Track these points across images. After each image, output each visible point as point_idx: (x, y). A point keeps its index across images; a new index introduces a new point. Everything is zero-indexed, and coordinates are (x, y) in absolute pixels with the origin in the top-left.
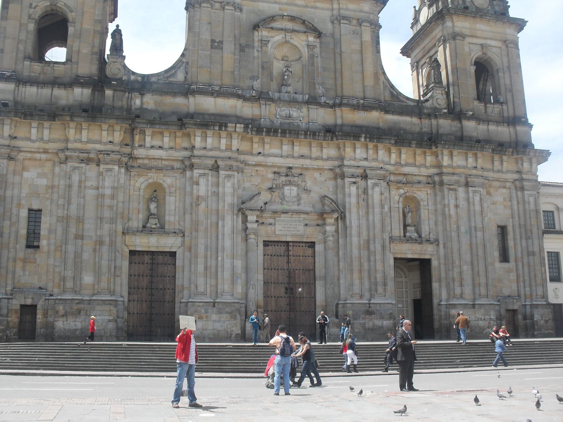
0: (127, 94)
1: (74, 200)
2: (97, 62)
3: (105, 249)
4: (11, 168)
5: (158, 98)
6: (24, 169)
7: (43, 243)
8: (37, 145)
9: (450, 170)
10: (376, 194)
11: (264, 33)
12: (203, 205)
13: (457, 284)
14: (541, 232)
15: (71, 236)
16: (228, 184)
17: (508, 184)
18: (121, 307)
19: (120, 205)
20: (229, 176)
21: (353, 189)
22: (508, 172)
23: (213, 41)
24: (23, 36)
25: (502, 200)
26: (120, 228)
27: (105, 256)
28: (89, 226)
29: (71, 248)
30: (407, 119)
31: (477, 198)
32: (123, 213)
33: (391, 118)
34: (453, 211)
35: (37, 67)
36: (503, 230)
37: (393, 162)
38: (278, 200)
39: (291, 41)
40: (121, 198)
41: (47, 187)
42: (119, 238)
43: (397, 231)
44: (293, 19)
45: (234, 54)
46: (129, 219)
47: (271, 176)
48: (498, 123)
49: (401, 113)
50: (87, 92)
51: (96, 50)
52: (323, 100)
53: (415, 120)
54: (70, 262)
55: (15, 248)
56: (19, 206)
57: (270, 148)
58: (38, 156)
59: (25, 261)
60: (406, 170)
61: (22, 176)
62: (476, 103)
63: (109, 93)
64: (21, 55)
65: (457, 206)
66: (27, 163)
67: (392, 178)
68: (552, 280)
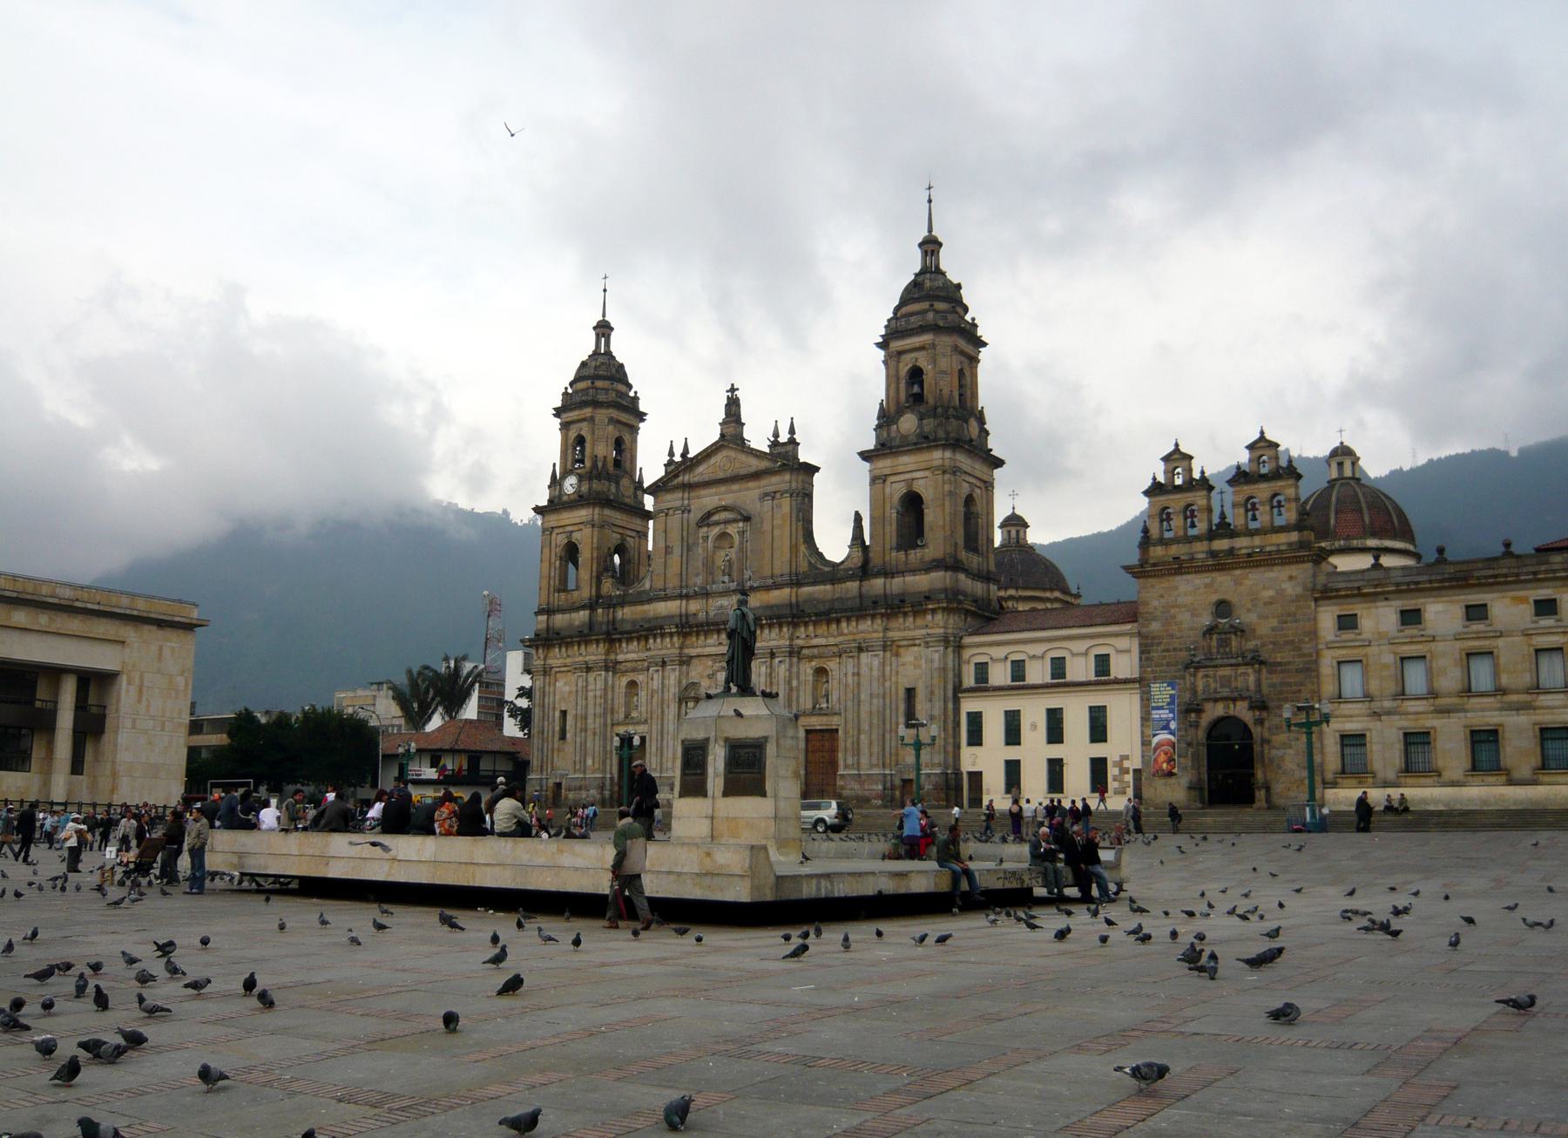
0: (611, 610)
1: (579, 702)
2: (594, 585)
3: (597, 738)
4: (547, 681)
5: (633, 608)
6: (556, 681)
7: (568, 735)
8: (560, 661)
9: (850, 637)
10: (782, 671)
11: (705, 529)
12: (655, 698)
13: (849, 754)
14: (950, 693)
15: (578, 730)
16: (672, 677)
17: (917, 642)
18: (608, 783)
19: (609, 702)
20: (674, 670)
21: (763, 668)
22: (915, 628)
23: (667, 547)
24: (552, 574)
25: (912, 659)
26: (609, 721)
27: (597, 744)
28: (590, 721)
29: (578, 740)
30: (821, 588)
31: (876, 663)
32: (612, 709)
33: (806, 590)
34: (850, 680)
35: (563, 595)
36: (910, 693)
37: (803, 636)
38: (713, 685)
39: (727, 531)
40: (610, 697)
41: (570, 692)
42: (609, 729)
43: (809, 705)
44: (725, 509)
45: (682, 556)
46: (618, 712)
47: (710, 663)
48: (914, 571)
49: (814, 583)
50: (587, 612)
51: (594, 574)
52: (749, 584)
53: (828, 587)
54: (578, 750)
55: (553, 742)
56: (554, 709)
57: (706, 638)
58: (562, 669)
59: (559, 750)
60: (815, 642)
61: (555, 685)
62: (894, 554)
63: (600, 611)
64: (552, 589)
65: (853, 674)
66: (558, 675)
67: (805, 652)
68: (970, 744)
